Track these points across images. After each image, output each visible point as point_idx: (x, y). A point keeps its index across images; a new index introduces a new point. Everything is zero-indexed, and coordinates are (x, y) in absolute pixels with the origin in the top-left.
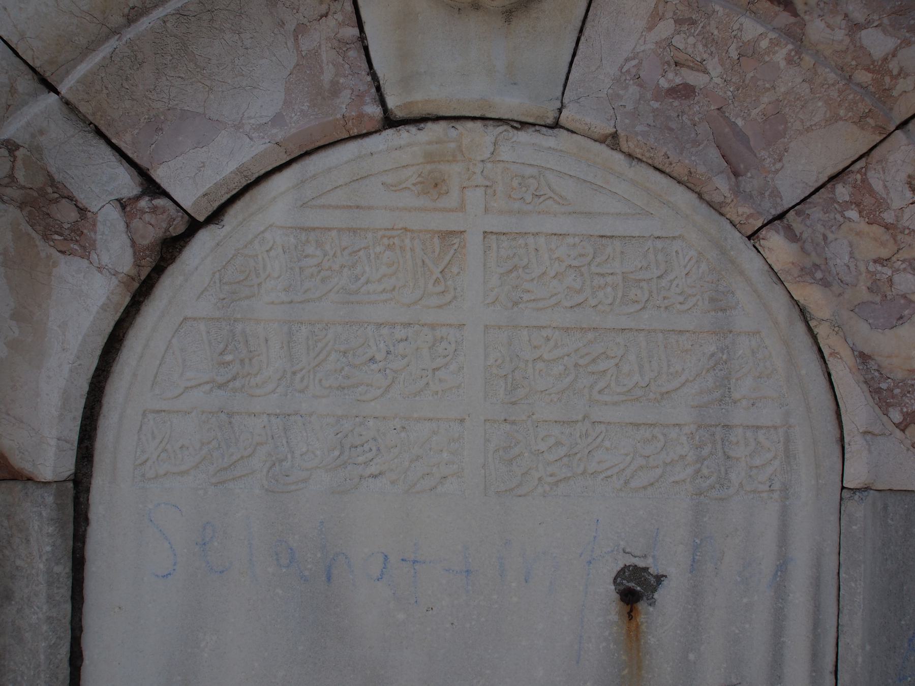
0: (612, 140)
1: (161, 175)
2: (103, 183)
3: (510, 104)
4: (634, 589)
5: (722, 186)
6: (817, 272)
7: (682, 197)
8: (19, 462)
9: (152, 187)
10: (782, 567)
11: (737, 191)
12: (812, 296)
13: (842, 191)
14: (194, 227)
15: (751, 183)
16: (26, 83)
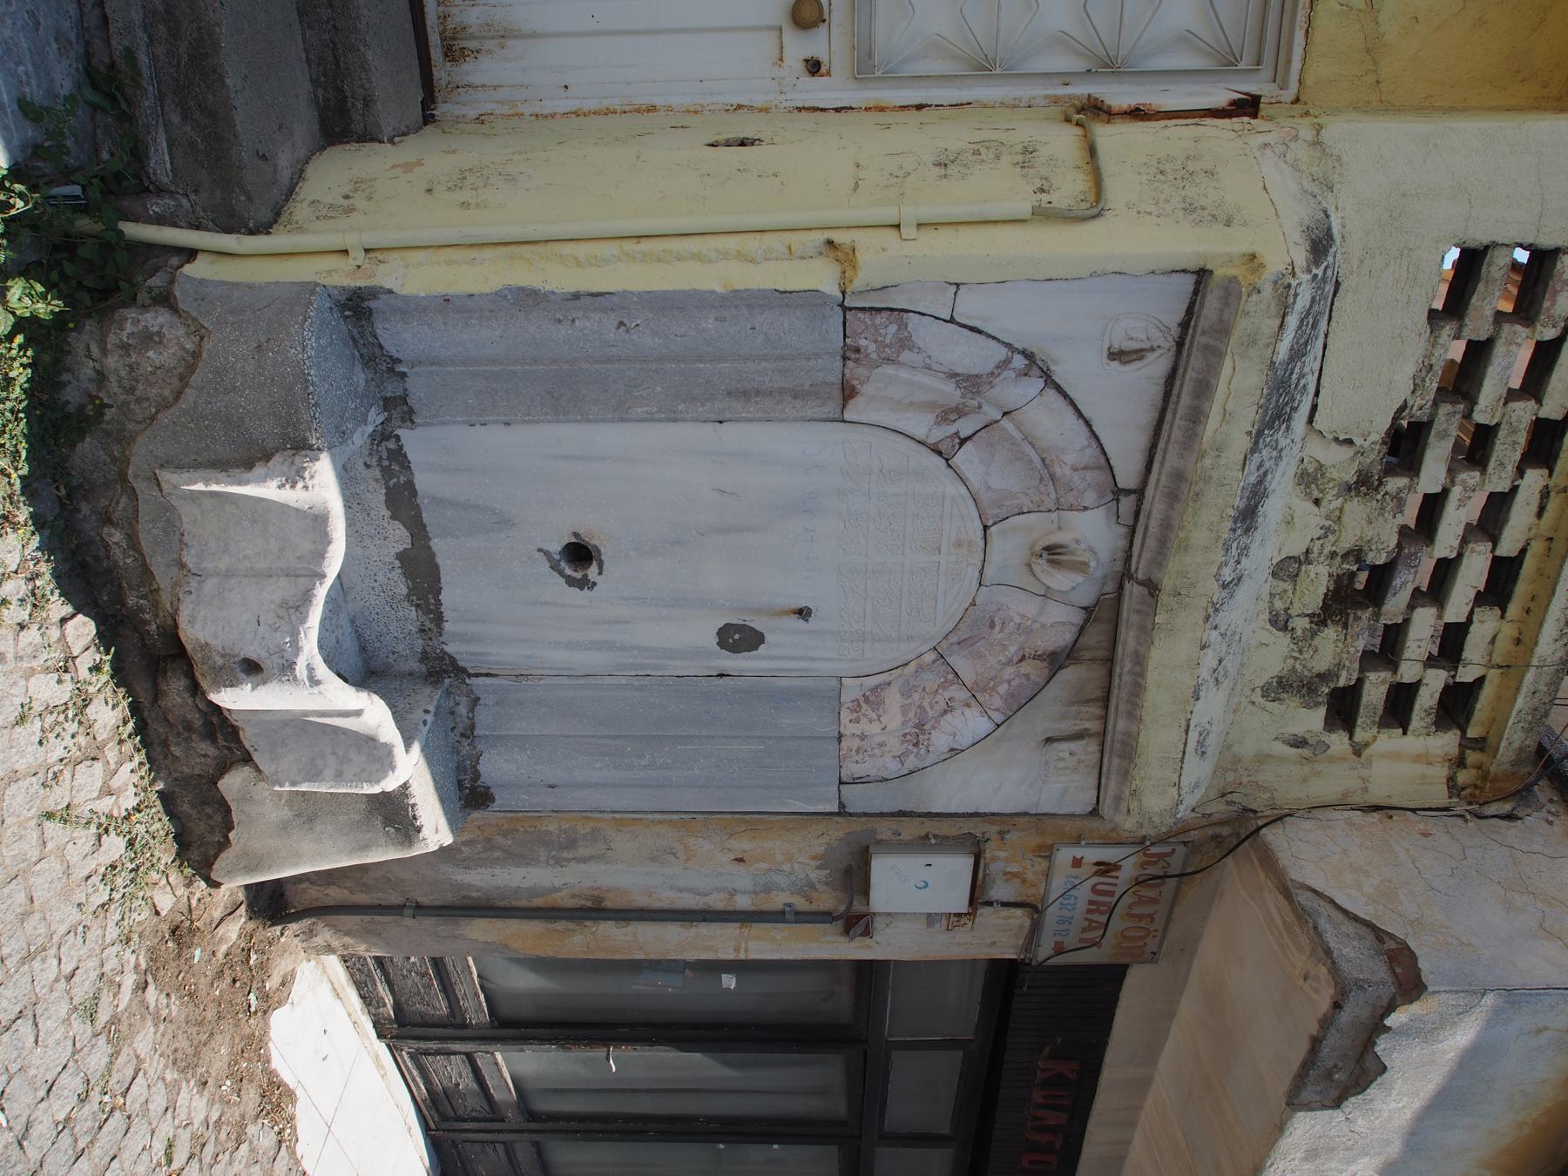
0: (973, 604)
1: (968, 445)
2: (965, 427)
3: (989, 571)
4: (803, 613)
5: (954, 639)
6: (921, 669)
7: (951, 626)
8: (851, 403)
9: (963, 442)
10: (812, 659)
12: (912, 667)
13: (951, 676)
15: (955, 648)
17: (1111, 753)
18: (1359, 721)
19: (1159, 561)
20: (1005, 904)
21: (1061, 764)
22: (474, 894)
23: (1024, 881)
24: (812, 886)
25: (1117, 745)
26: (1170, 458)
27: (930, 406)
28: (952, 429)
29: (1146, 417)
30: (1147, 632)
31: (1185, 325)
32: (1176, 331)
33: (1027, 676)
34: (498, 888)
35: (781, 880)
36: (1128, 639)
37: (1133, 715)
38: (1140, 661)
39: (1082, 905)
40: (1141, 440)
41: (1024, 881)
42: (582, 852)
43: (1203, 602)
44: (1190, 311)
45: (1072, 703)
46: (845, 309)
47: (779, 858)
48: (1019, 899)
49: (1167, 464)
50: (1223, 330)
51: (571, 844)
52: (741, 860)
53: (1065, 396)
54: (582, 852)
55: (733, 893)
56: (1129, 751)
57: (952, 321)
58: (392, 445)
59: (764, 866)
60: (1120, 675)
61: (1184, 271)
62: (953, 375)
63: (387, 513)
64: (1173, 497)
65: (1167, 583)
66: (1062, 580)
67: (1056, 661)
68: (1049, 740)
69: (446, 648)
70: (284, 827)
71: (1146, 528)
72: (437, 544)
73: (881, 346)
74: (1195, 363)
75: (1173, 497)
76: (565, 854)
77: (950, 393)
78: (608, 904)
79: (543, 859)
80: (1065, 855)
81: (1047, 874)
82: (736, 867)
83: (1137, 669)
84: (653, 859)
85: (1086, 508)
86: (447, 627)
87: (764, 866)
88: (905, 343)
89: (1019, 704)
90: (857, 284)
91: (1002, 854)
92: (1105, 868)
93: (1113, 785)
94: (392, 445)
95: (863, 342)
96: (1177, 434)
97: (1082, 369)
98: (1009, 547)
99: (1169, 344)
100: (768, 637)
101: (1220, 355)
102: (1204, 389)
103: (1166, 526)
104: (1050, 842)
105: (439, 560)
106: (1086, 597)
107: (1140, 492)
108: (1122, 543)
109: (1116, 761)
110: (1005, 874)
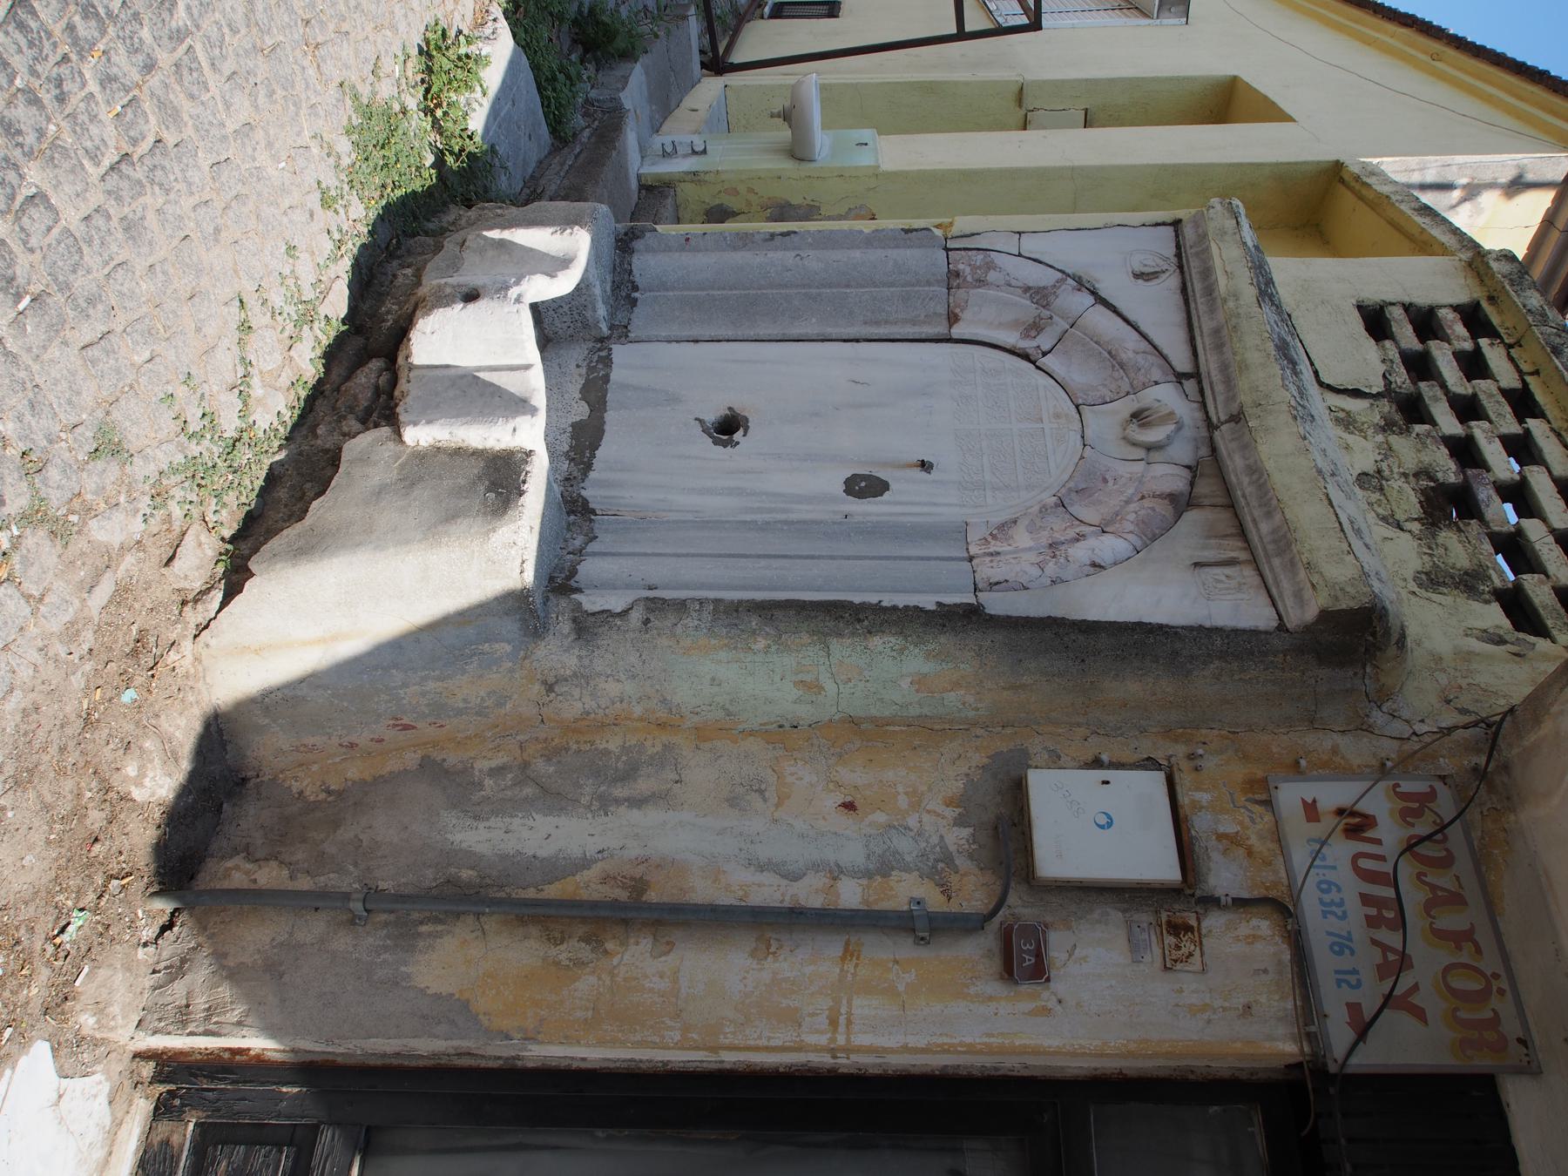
0: (1082, 457)
4: (925, 466)
11: (1070, 490)
14: (1034, 363)
16: (1071, 321)
17: (1269, 562)
18: (1549, 623)
19: (1231, 397)
20: (1240, 903)
21: (1220, 586)
22: (466, 874)
23: (1250, 853)
24: (948, 859)
25: (1270, 547)
26: (1205, 324)
27: (1014, 324)
28: (1034, 344)
29: (1178, 317)
30: (1247, 447)
31: (1179, 255)
32: (1174, 260)
33: (1153, 509)
34: (504, 857)
35: (905, 846)
36: (1235, 463)
37: (1269, 502)
38: (1256, 471)
39: (1356, 912)
40: (1180, 335)
41: (1250, 853)
42: (643, 786)
43: (1285, 407)
44: (1178, 246)
45: (1209, 537)
46: (947, 250)
47: (903, 802)
48: (1256, 894)
49: (1205, 330)
50: (1203, 237)
51: (629, 774)
52: (849, 806)
53: (1115, 311)
54: (643, 786)
55: (836, 872)
56: (1285, 541)
57: (1020, 255)
58: (603, 354)
59: (881, 817)
60: (1244, 496)
61: (1164, 224)
62: (1027, 289)
63: (578, 396)
64: (1219, 347)
65: (1245, 398)
66: (1154, 435)
67: (1181, 503)
68: (1196, 565)
69: (583, 493)
70: (380, 492)
71: (1211, 384)
72: (610, 416)
73: (974, 268)
74: (1194, 266)
75: (1219, 347)
76: (619, 792)
77: (1027, 309)
78: (652, 896)
79: (585, 800)
80: (1290, 795)
81: (1278, 836)
82: (844, 822)
83: (1255, 477)
84: (733, 802)
85: (1156, 383)
86: (592, 475)
87: (881, 817)
88: (990, 266)
89: (1151, 535)
90: (955, 231)
91: (1204, 797)
92: (1356, 824)
93: (1286, 586)
94: (603, 354)
95: (961, 267)
96: (1202, 308)
97: (1115, 285)
98: (1106, 423)
99: (1173, 268)
100: (893, 486)
101: (1207, 250)
102: (1207, 273)
103: (1224, 368)
104: (1260, 774)
105: (607, 427)
106: (1183, 451)
107: (1196, 375)
108: (1199, 415)
109: (1276, 562)
110: (1221, 837)
